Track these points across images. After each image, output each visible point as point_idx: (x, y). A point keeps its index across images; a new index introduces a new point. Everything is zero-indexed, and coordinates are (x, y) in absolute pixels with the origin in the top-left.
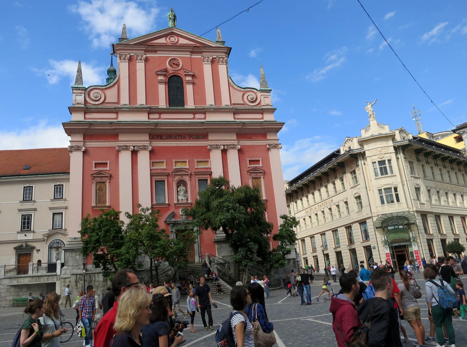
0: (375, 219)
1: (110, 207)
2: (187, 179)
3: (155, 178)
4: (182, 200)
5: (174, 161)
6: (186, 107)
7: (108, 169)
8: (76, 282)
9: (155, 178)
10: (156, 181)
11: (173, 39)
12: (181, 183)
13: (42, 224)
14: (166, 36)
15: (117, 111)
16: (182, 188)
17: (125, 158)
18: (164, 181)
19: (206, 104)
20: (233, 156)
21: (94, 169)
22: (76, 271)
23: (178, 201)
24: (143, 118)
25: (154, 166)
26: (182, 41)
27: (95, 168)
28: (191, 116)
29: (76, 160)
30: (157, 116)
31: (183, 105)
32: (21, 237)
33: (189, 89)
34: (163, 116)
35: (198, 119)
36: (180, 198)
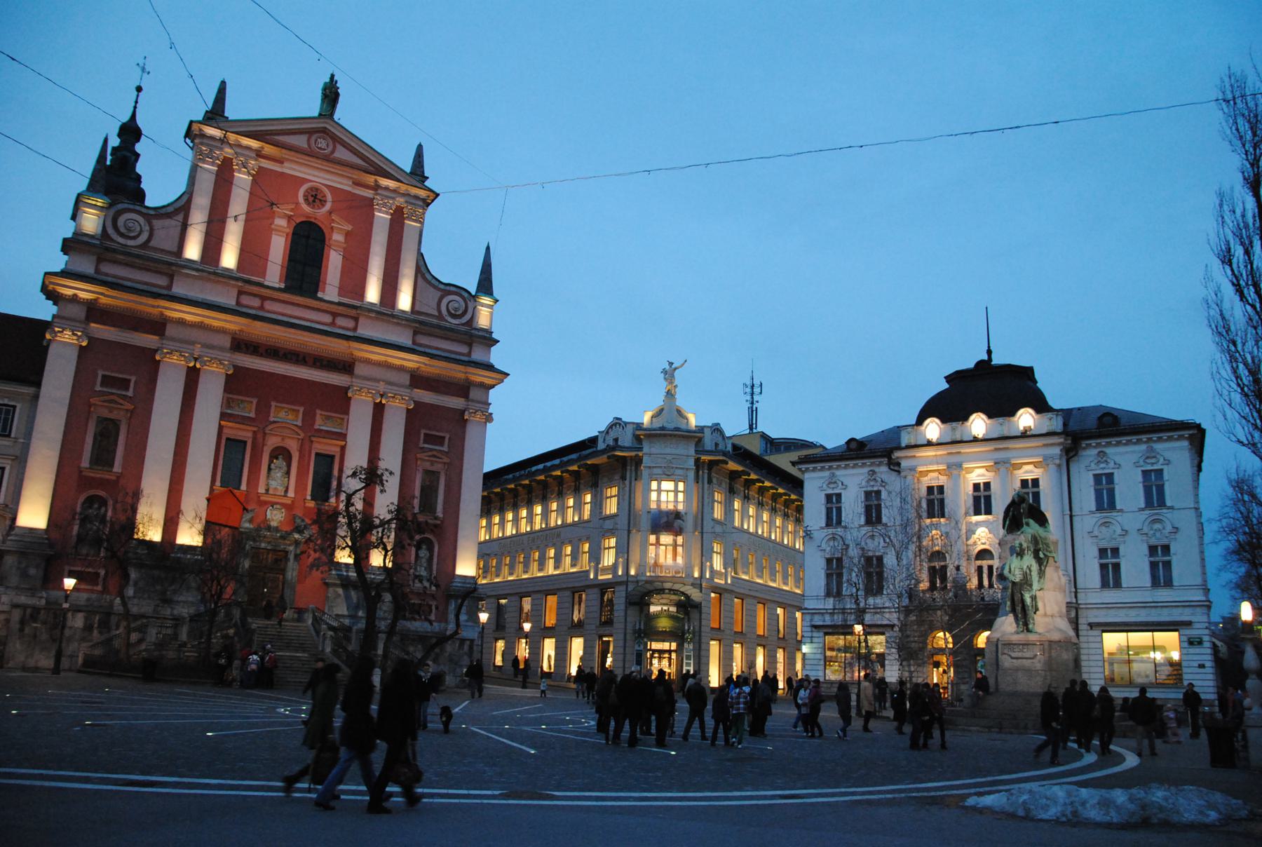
0: (631, 587)
1: (119, 476)
2: (293, 446)
4: (276, 489)
5: (273, 404)
6: (320, 295)
7: (130, 393)
8: (22, 622)
10: (228, 439)
11: (322, 143)
12: (281, 453)
16: (280, 462)
18: (245, 442)
21: (98, 388)
22: (23, 599)
23: (267, 490)
25: (229, 407)
26: (341, 153)
27: (102, 385)
28: (328, 319)
30: (256, 302)
33: (334, 262)
34: (269, 305)
35: (340, 327)
36: (273, 484)
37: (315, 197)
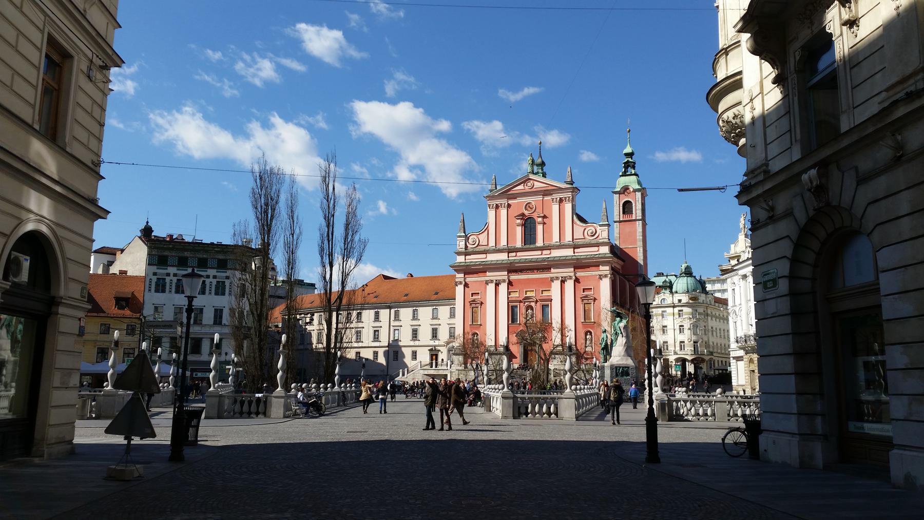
3: (511, 304)
9: (511, 304)
11: (529, 184)
13: (443, 335)
14: (524, 182)
15: (485, 252)
17: (491, 288)
19: (552, 240)
20: (569, 285)
24: (503, 257)
28: (539, 252)
29: (460, 290)
30: (514, 254)
31: (535, 243)
32: (432, 343)
33: (540, 228)
34: (519, 254)
37: (528, 206)
